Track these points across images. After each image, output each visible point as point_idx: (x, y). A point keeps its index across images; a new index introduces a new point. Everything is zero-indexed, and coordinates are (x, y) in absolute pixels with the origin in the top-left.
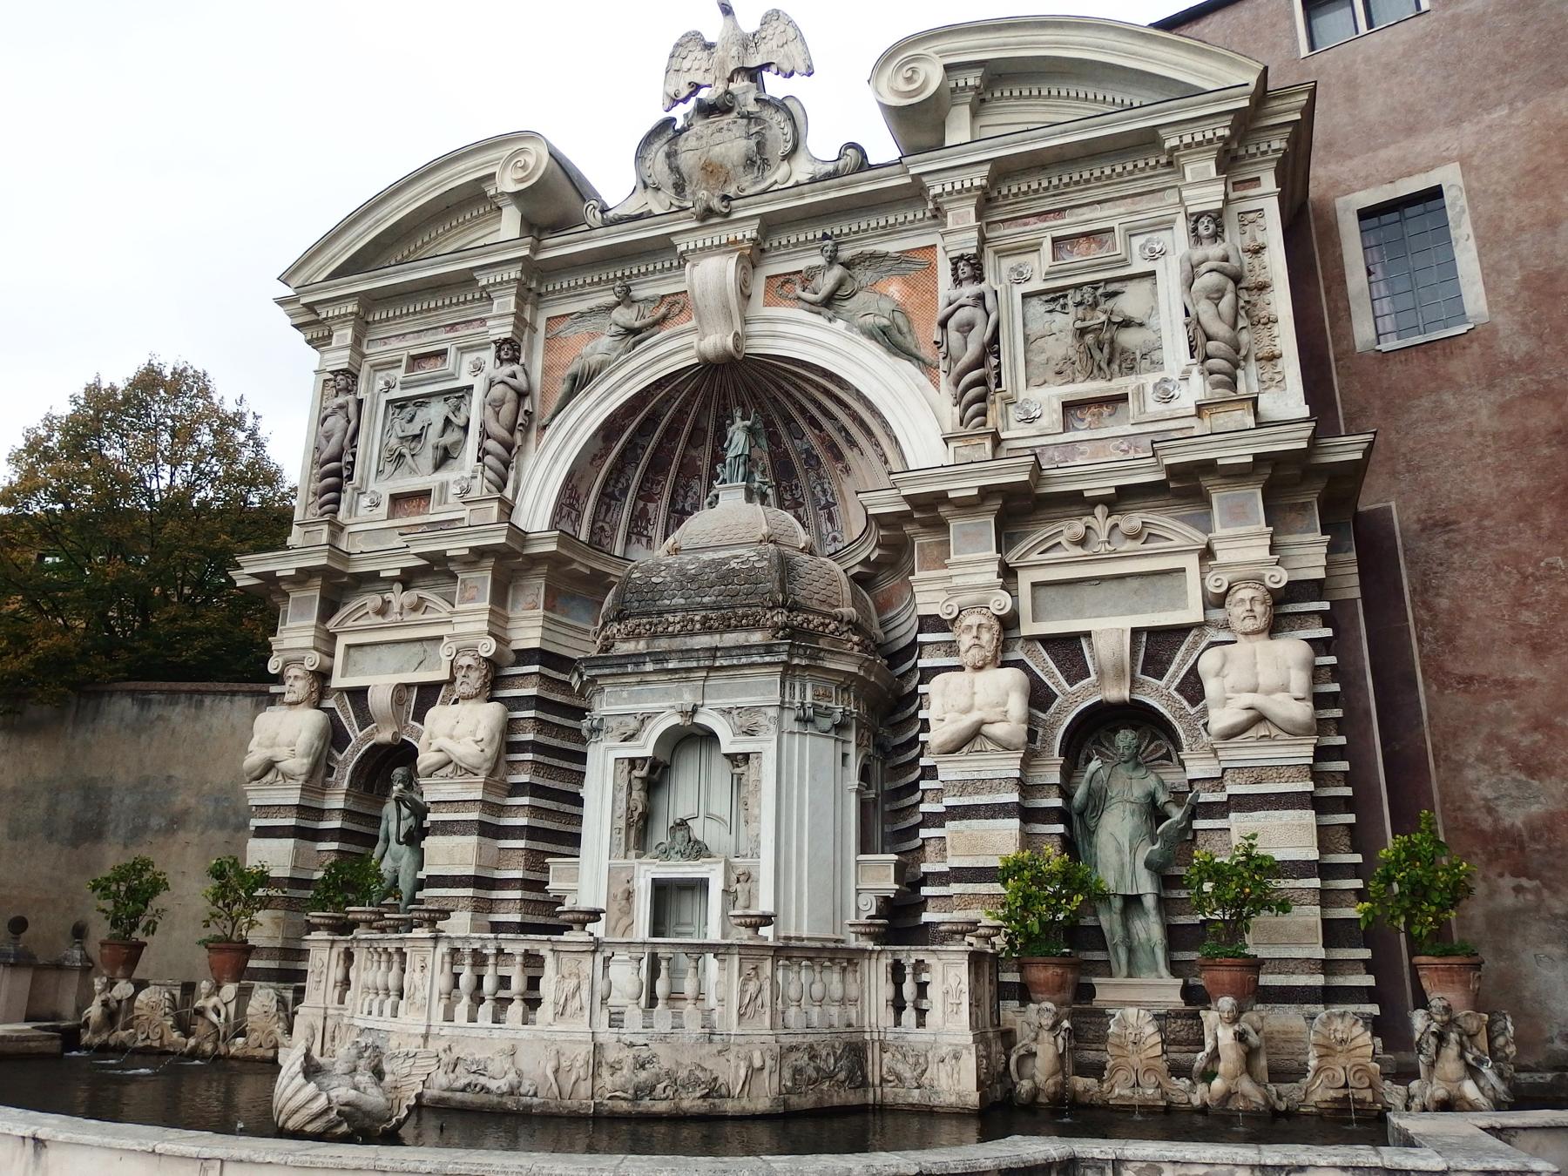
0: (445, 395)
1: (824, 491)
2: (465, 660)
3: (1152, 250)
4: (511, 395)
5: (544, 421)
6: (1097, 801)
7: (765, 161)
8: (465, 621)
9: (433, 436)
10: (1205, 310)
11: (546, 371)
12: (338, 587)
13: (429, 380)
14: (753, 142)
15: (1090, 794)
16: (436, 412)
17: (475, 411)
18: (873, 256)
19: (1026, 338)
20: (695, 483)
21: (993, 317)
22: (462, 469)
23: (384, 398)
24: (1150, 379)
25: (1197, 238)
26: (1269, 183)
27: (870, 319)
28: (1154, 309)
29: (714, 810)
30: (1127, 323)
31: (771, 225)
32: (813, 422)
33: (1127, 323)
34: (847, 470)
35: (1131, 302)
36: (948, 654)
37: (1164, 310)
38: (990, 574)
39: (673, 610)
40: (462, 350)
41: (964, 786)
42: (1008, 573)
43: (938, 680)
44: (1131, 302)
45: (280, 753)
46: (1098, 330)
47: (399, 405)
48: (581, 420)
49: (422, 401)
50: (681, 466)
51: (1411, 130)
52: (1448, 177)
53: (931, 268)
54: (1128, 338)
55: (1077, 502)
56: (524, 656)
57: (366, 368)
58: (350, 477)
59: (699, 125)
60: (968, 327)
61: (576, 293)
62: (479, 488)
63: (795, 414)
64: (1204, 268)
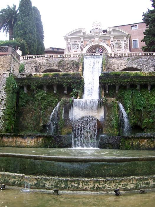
0: (77, 44)
10: (125, 46)
16: (76, 46)
18: (107, 40)
26: (129, 39)
31: (100, 37)
37: (123, 45)
44: (121, 45)
47: (73, 45)
49: (75, 45)
51: (136, 36)
52: (138, 39)
60: (112, 45)
61: (87, 39)
62: (81, 51)
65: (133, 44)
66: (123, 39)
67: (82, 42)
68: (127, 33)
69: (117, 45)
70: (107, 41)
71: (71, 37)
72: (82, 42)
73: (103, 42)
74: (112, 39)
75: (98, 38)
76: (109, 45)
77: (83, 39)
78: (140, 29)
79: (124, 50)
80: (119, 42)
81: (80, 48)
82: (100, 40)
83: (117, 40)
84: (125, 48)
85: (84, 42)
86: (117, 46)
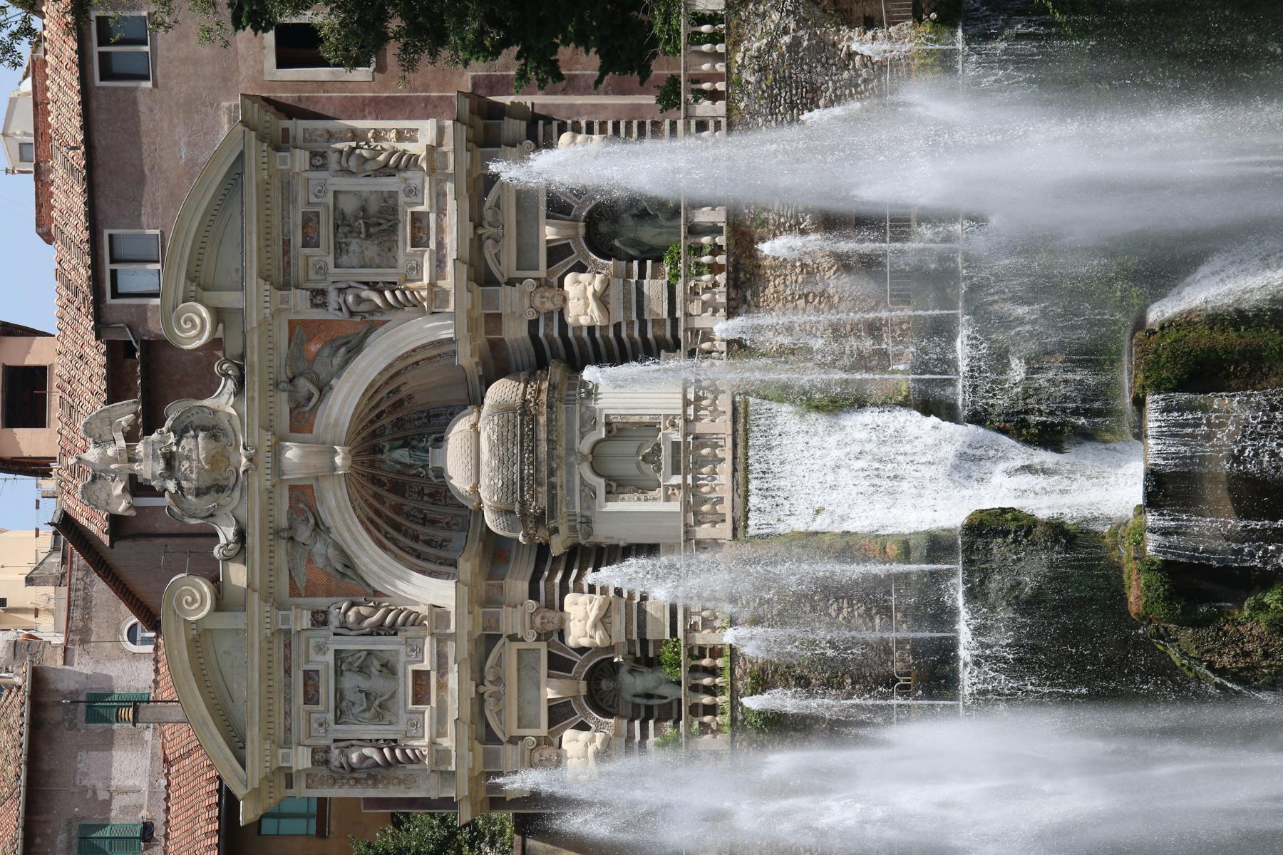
0: (339, 673)
1: (419, 418)
2: (538, 620)
3: (320, 191)
4: (354, 609)
5: (370, 591)
6: (636, 243)
7: (214, 427)
8: (517, 616)
14: (201, 435)
15: (632, 246)
16: (351, 681)
19: (362, 267)
20: (406, 509)
21: (353, 284)
22: (397, 652)
23: (333, 726)
24: (402, 199)
25: (323, 167)
26: (287, 123)
27: (337, 361)
28: (356, 193)
29: (634, 451)
30: (364, 209)
32: (379, 416)
33: (364, 209)
34: (410, 397)
35: (349, 206)
36: (551, 319)
39: (522, 471)
40: (308, 662)
41: (627, 308)
42: (511, 282)
43: (570, 320)
44: (349, 206)
45: (591, 749)
46: (367, 225)
48: (374, 561)
49: (339, 694)
50: (395, 512)
53: (306, 324)
54: (373, 208)
55: (477, 244)
56: (534, 594)
57: (308, 742)
58: (395, 741)
60: (358, 297)
63: (373, 428)
64: (344, 164)
72: (320, 619)
73: (320, 400)
75: (277, 451)
80: (326, 232)
81: (383, 644)
83: (300, 253)
85: (311, 591)
86: (372, 250)
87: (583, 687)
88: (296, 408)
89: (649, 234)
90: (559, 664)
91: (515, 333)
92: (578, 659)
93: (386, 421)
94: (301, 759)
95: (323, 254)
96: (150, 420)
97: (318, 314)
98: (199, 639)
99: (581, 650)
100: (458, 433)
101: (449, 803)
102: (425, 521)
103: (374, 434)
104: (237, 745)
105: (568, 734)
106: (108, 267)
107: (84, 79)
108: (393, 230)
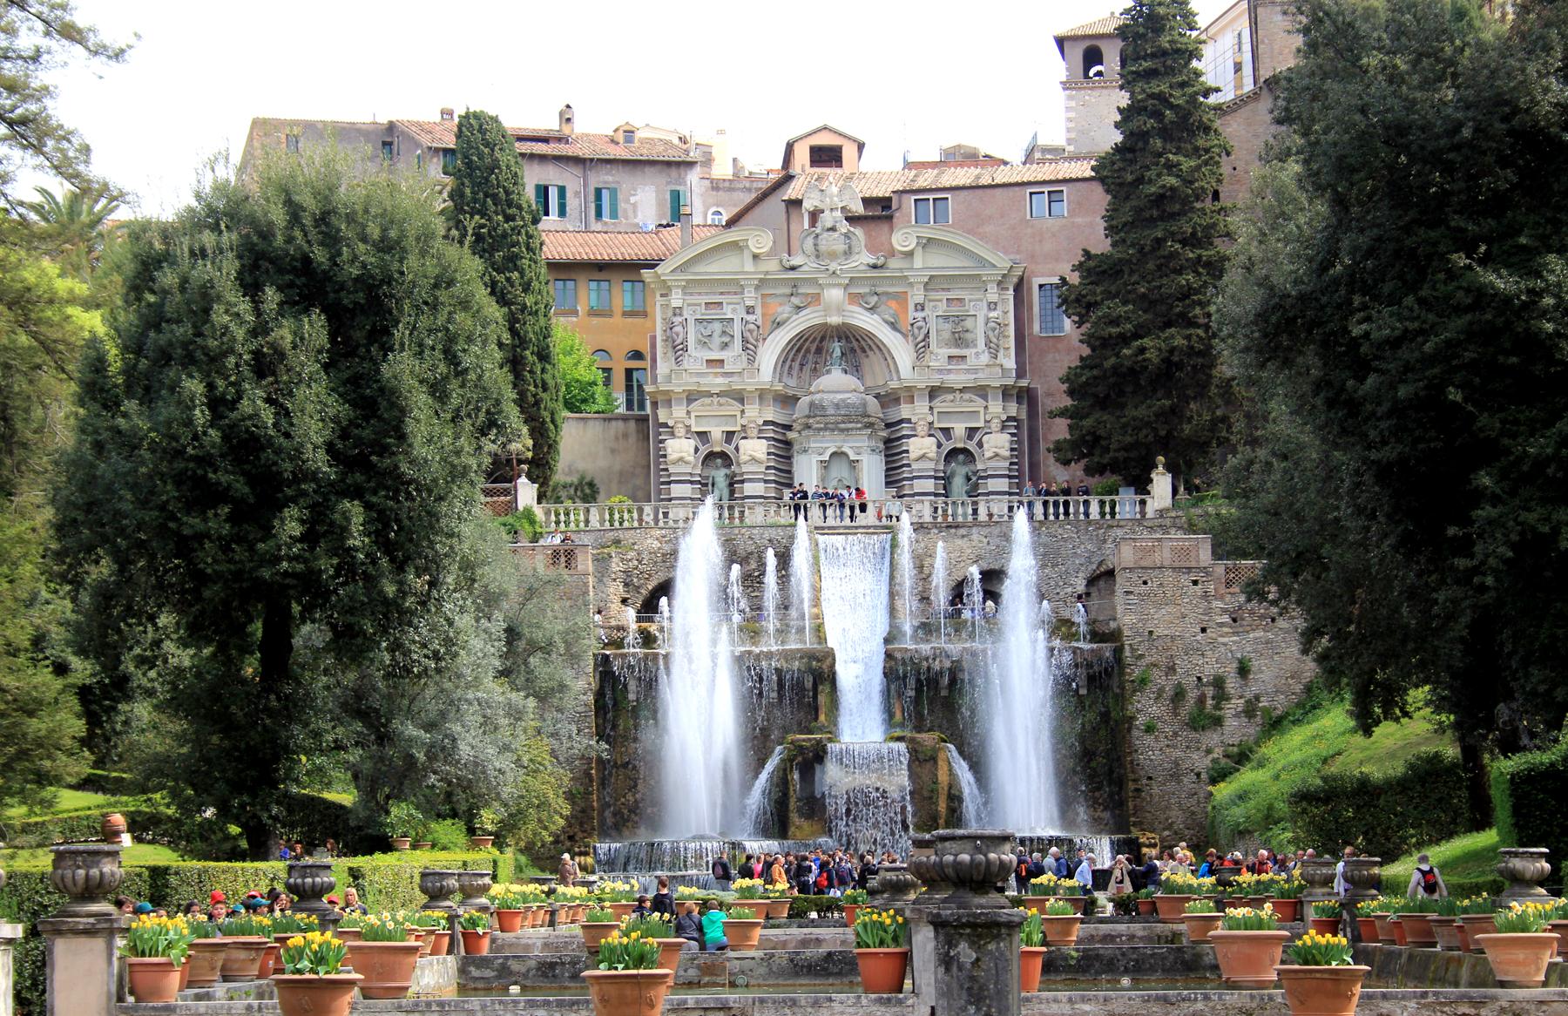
6: (953, 474)
9: (716, 335)
10: (991, 334)
11: (764, 315)
12: (691, 397)
13: (713, 314)
16: (717, 327)
17: (737, 329)
38: (926, 410)
44: (969, 323)
49: (710, 321)
51: (1057, 260)
54: (968, 336)
55: (952, 390)
56: (766, 423)
59: (825, 235)
60: (920, 328)
65: (1036, 309)
66: (978, 295)
67: (750, 310)
68: (1002, 262)
69: (948, 326)
70: (893, 304)
71: (688, 281)
72: (750, 310)
74: (917, 295)
75: (839, 285)
76: (906, 327)
77: (757, 288)
78: (1079, 220)
79: (985, 358)
80: (955, 310)
82: (855, 298)
83: (944, 296)
84: (993, 349)
85: (764, 305)
86: (947, 335)
87: (717, 449)
88: (862, 296)
89: (958, 483)
90: (729, 435)
91: (905, 411)
92: (732, 447)
93: (855, 344)
94: (676, 300)
95: (942, 308)
96: (852, 219)
97: (911, 307)
98: (736, 246)
99: (737, 449)
100: (850, 381)
101: (655, 381)
102: (802, 365)
103: (847, 338)
104: (682, 268)
105: (692, 443)
106: (931, 197)
107: (1030, 183)
108: (957, 346)
